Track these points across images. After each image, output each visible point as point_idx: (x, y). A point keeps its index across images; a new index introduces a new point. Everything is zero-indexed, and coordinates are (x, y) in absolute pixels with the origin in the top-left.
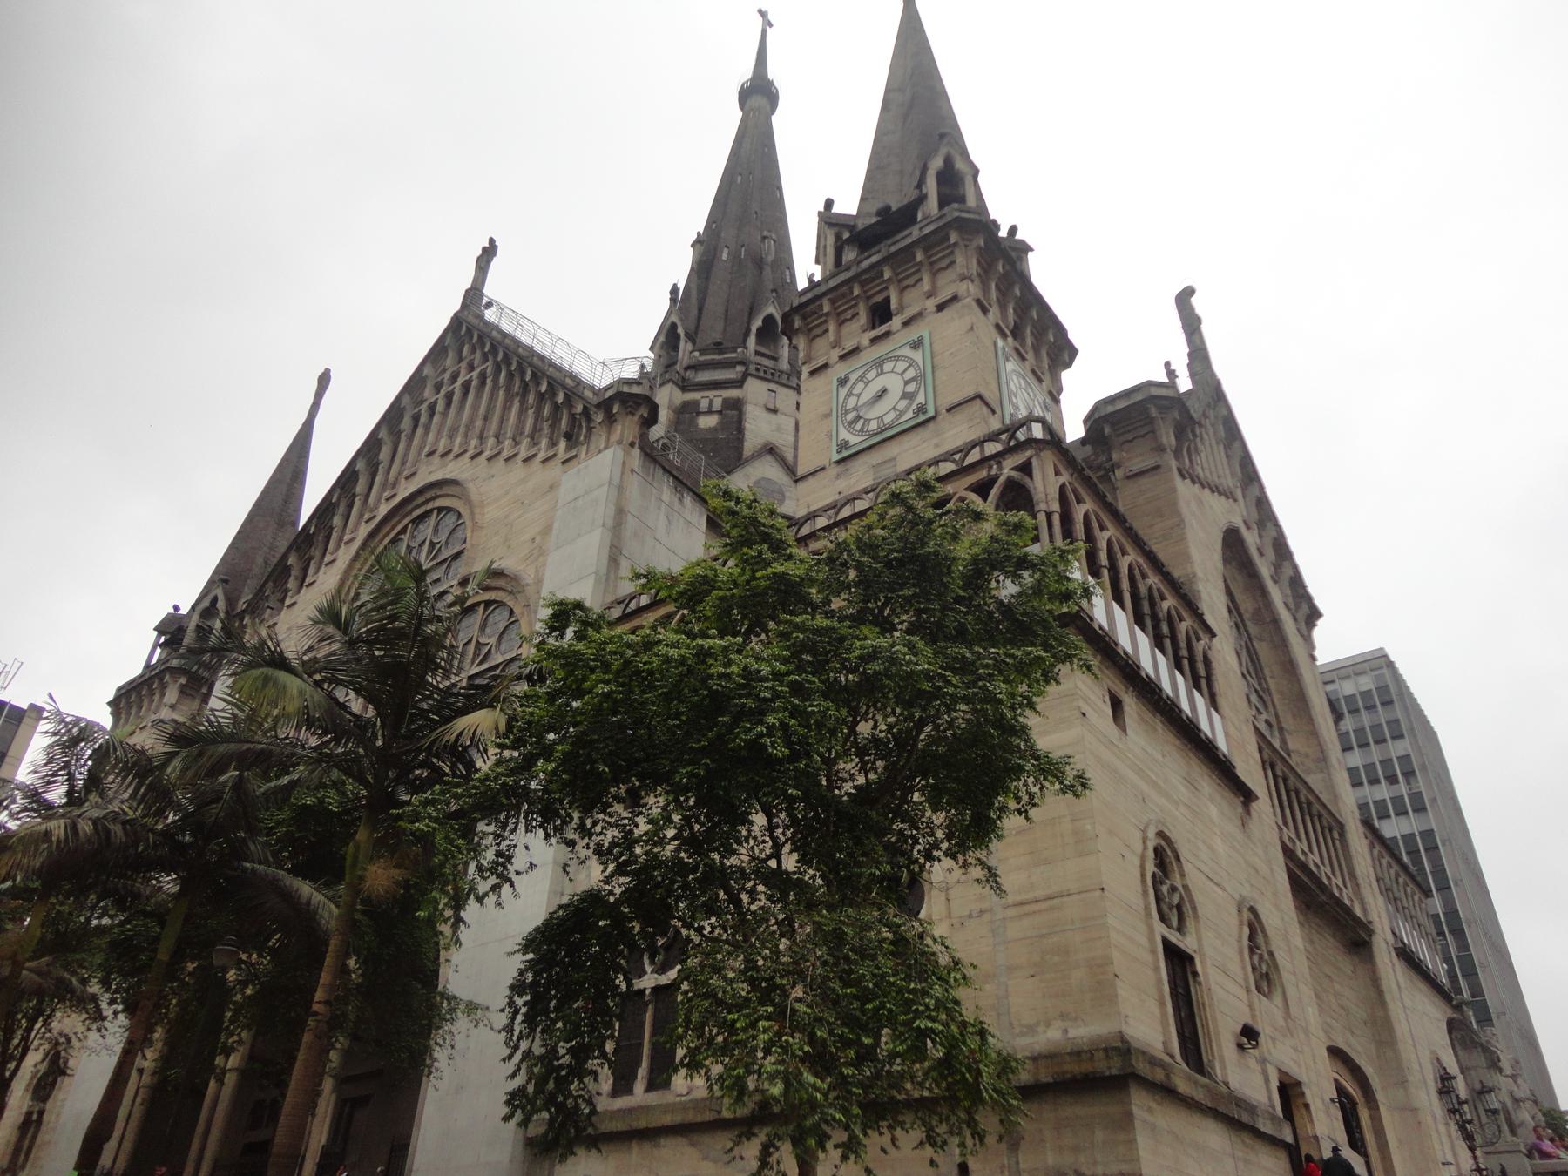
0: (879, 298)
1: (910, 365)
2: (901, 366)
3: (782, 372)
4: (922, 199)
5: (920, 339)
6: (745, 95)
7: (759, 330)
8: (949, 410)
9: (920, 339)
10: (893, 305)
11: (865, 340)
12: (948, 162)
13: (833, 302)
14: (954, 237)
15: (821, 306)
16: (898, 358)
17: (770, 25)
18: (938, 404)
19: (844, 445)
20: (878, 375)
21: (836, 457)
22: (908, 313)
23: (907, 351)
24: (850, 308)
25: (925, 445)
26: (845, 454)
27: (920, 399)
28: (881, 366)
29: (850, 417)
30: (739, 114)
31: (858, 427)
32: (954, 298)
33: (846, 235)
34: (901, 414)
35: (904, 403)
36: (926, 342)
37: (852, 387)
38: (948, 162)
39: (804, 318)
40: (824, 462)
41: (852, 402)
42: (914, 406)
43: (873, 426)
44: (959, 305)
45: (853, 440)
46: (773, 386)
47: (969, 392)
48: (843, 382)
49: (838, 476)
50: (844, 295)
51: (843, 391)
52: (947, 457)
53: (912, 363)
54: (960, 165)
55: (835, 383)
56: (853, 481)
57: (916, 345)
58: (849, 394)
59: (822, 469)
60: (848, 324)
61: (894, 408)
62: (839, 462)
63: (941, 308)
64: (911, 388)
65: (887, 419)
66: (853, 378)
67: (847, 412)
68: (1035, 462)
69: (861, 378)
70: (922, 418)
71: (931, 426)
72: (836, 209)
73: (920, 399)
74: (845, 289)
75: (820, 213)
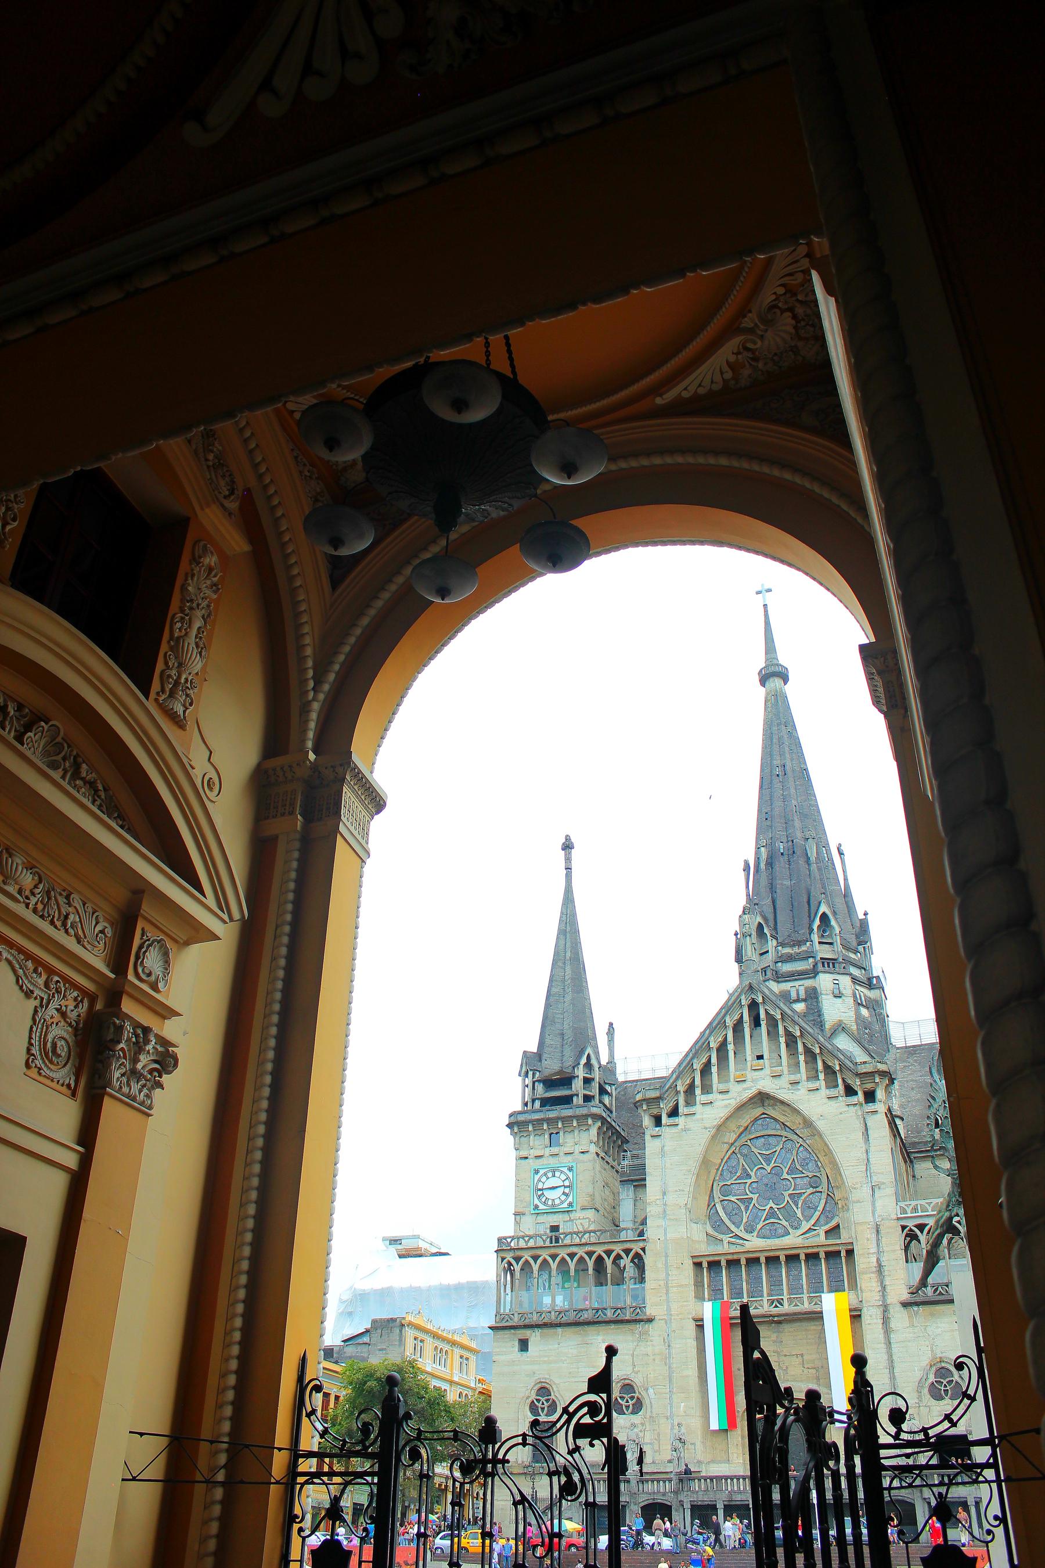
11: (547, 1151)
12: (589, 1056)
19: (536, 1207)
23: (565, 1170)
26: (537, 1212)
27: (570, 1199)
31: (543, 1200)
34: (562, 1202)
35: (563, 1197)
36: (574, 1169)
38: (589, 1056)
42: (567, 1202)
43: (550, 1203)
45: (541, 1207)
48: (537, 1172)
51: (537, 1177)
55: (533, 1172)
57: (570, 1169)
64: (567, 1190)
66: (542, 1172)
69: (545, 1174)
73: (570, 1199)
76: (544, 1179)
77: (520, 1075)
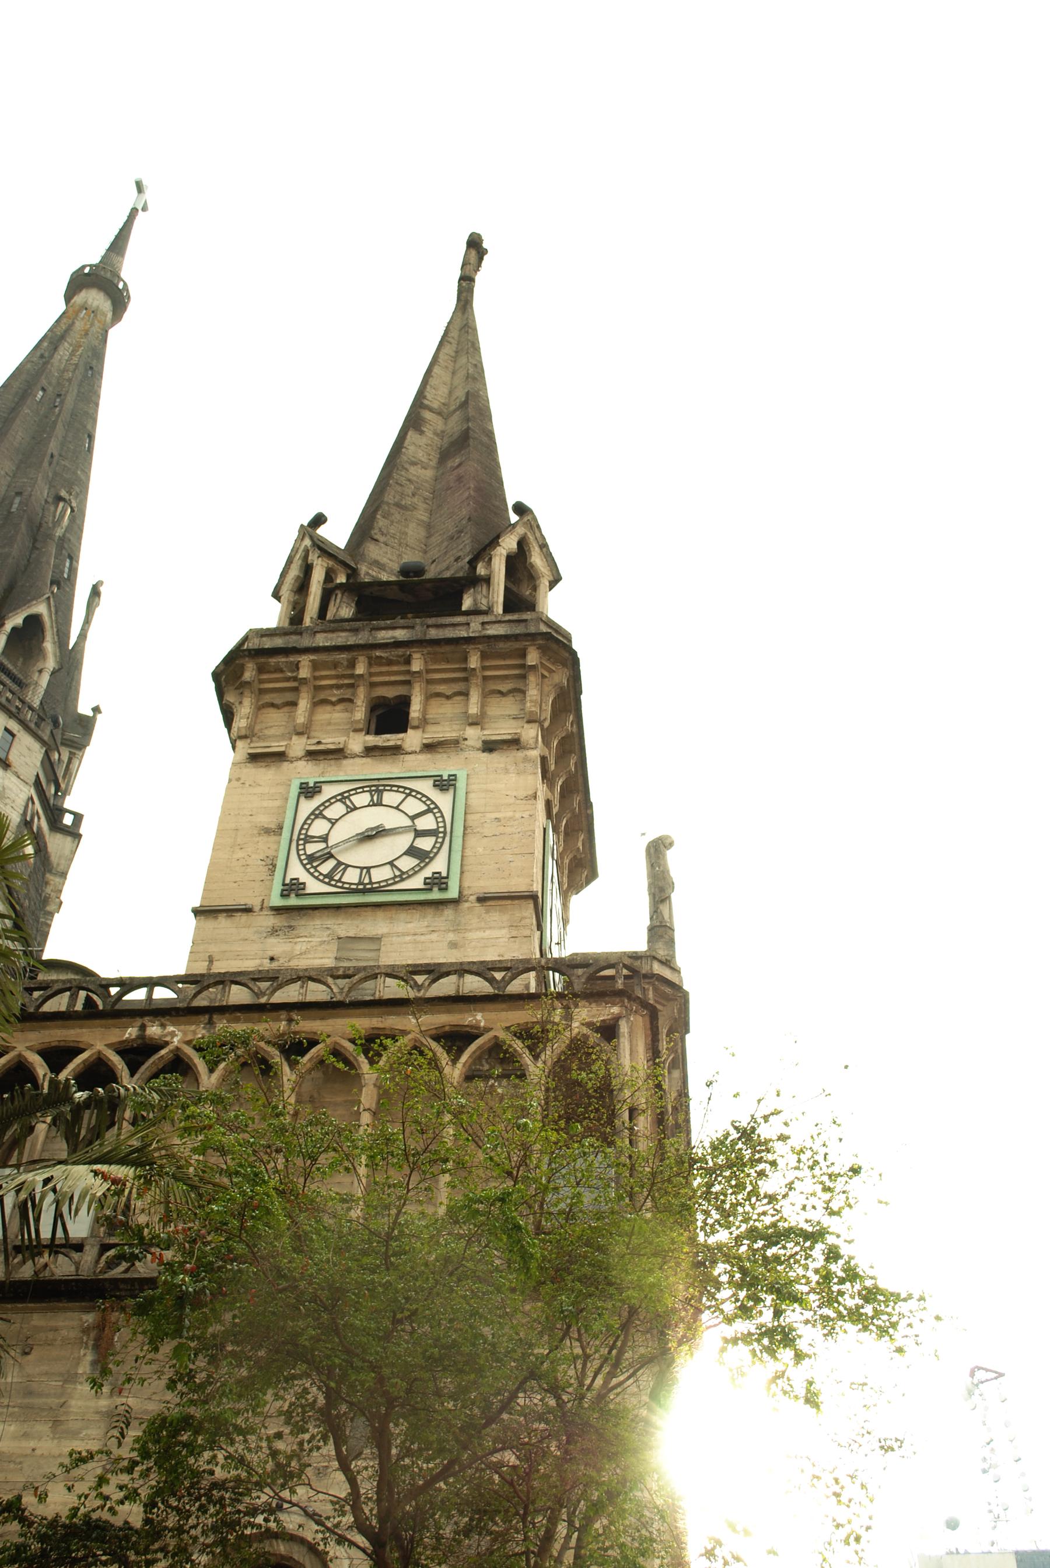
0: (390, 693)
1: (429, 811)
2: (413, 806)
3: (31, 708)
4: (474, 581)
5: (453, 778)
6: (80, 281)
7: (14, 629)
8: (482, 900)
9: (453, 778)
10: (415, 710)
11: (357, 743)
13: (315, 666)
14: (533, 657)
15: (297, 667)
16: (410, 793)
17: (145, 209)
18: (466, 884)
19: (293, 887)
20: (373, 804)
21: (276, 901)
22: (435, 733)
23: (425, 787)
24: (338, 687)
25: (434, 937)
26: (293, 901)
27: (439, 865)
28: (381, 793)
29: (312, 848)
30: (62, 307)
31: (326, 868)
32: (515, 743)
33: (341, 579)
34: (403, 876)
35: (407, 863)
36: (461, 784)
37: (329, 802)
39: (261, 670)
40: (255, 902)
41: (319, 828)
42: (428, 872)
43: (352, 877)
44: (520, 754)
45: (314, 886)
46: (14, 726)
47: (517, 884)
48: (308, 791)
49: (274, 932)
50: (335, 665)
51: (307, 807)
52: (483, 970)
53: (431, 809)
54: (536, 559)
55: (295, 790)
56: (299, 948)
57: (444, 784)
58: (317, 814)
59: (248, 910)
60: (329, 708)
61: (391, 863)
62: (278, 910)
63: (489, 747)
64: (425, 844)
65: (380, 875)
66: (329, 792)
67: (308, 839)
68: (624, 1027)
69: (343, 798)
70: (436, 895)
71: (449, 912)
72: (322, 531)
73: (439, 865)
74: (343, 656)
75: (302, 526)
76: (336, 810)
77: (276, 595)
